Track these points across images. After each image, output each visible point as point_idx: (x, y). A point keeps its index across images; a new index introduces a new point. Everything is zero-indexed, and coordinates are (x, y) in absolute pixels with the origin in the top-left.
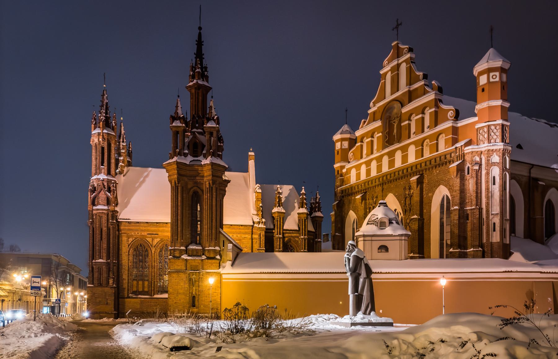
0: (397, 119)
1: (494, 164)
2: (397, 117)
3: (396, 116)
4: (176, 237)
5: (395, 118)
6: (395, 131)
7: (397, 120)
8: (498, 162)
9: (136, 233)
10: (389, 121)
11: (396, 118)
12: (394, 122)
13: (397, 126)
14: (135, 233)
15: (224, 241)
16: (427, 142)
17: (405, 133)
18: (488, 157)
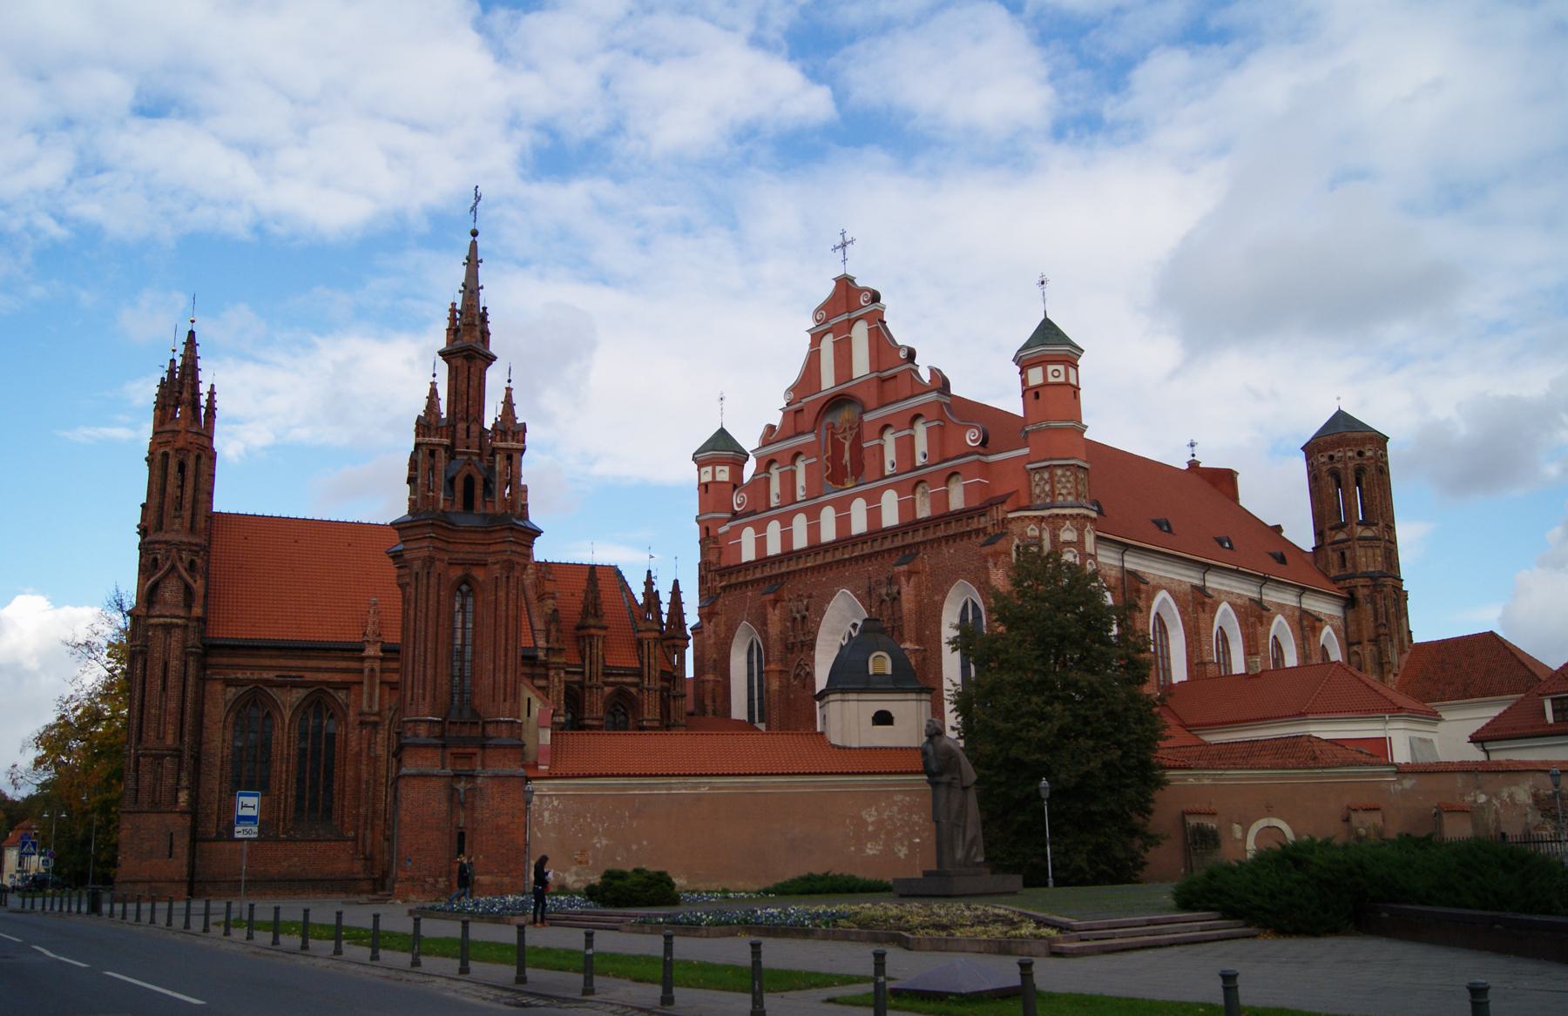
1: (1068, 543)
2: (851, 429)
3: (848, 425)
4: (421, 691)
5: (845, 429)
6: (847, 456)
8: (1075, 540)
9: (249, 673)
10: (833, 434)
11: (847, 429)
12: (845, 438)
13: (851, 446)
14: (246, 674)
15: (529, 699)
16: (923, 488)
17: (869, 462)
18: (1054, 529)
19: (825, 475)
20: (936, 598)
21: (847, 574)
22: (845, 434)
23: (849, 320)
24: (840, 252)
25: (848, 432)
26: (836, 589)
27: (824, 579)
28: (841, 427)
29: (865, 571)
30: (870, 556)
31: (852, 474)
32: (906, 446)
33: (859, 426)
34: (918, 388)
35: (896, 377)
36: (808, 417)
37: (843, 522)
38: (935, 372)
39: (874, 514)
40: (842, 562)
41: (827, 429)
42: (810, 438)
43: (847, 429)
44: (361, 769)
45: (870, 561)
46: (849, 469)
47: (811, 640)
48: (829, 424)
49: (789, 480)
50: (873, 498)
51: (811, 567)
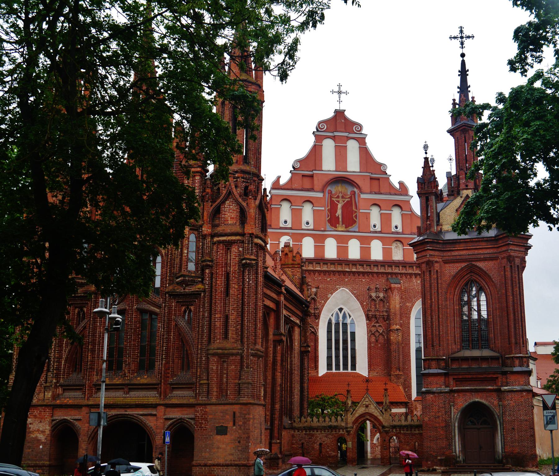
0: (344, 200)
3: (340, 195)
6: (339, 212)
7: (344, 201)
10: (331, 197)
11: (340, 198)
12: (338, 202)
13: (343, 207)
19: (327, 219)
20: (407, 304)
21: (346, 280)
22: (337, 199)
23: (347, 137)
24: (336, 95)
25: (340, 200)
26: (337, 287)
27: (329, 279)
28: (335, 194)
29: (359, 281)
30: (364, 273)
31: (343, 224)
32: (386, 219)
33: (351, 198)
34: (391, 190)
35: (379, 179)
36: (318, 183)
37: (343, 249)
38: (401, 184)
39: (365, 250)
40: (344, 273)
41: (329, 193)
42: (320, 195)
43: (340, 198)
44: (276, 375)
45: (363, 276)
46: (340, 220)
47: (318, 313)
48: (329, 190)
49: (297, 214)
50: (365, 242)
51: (320, 271)
